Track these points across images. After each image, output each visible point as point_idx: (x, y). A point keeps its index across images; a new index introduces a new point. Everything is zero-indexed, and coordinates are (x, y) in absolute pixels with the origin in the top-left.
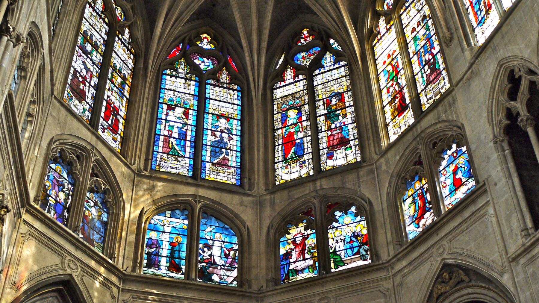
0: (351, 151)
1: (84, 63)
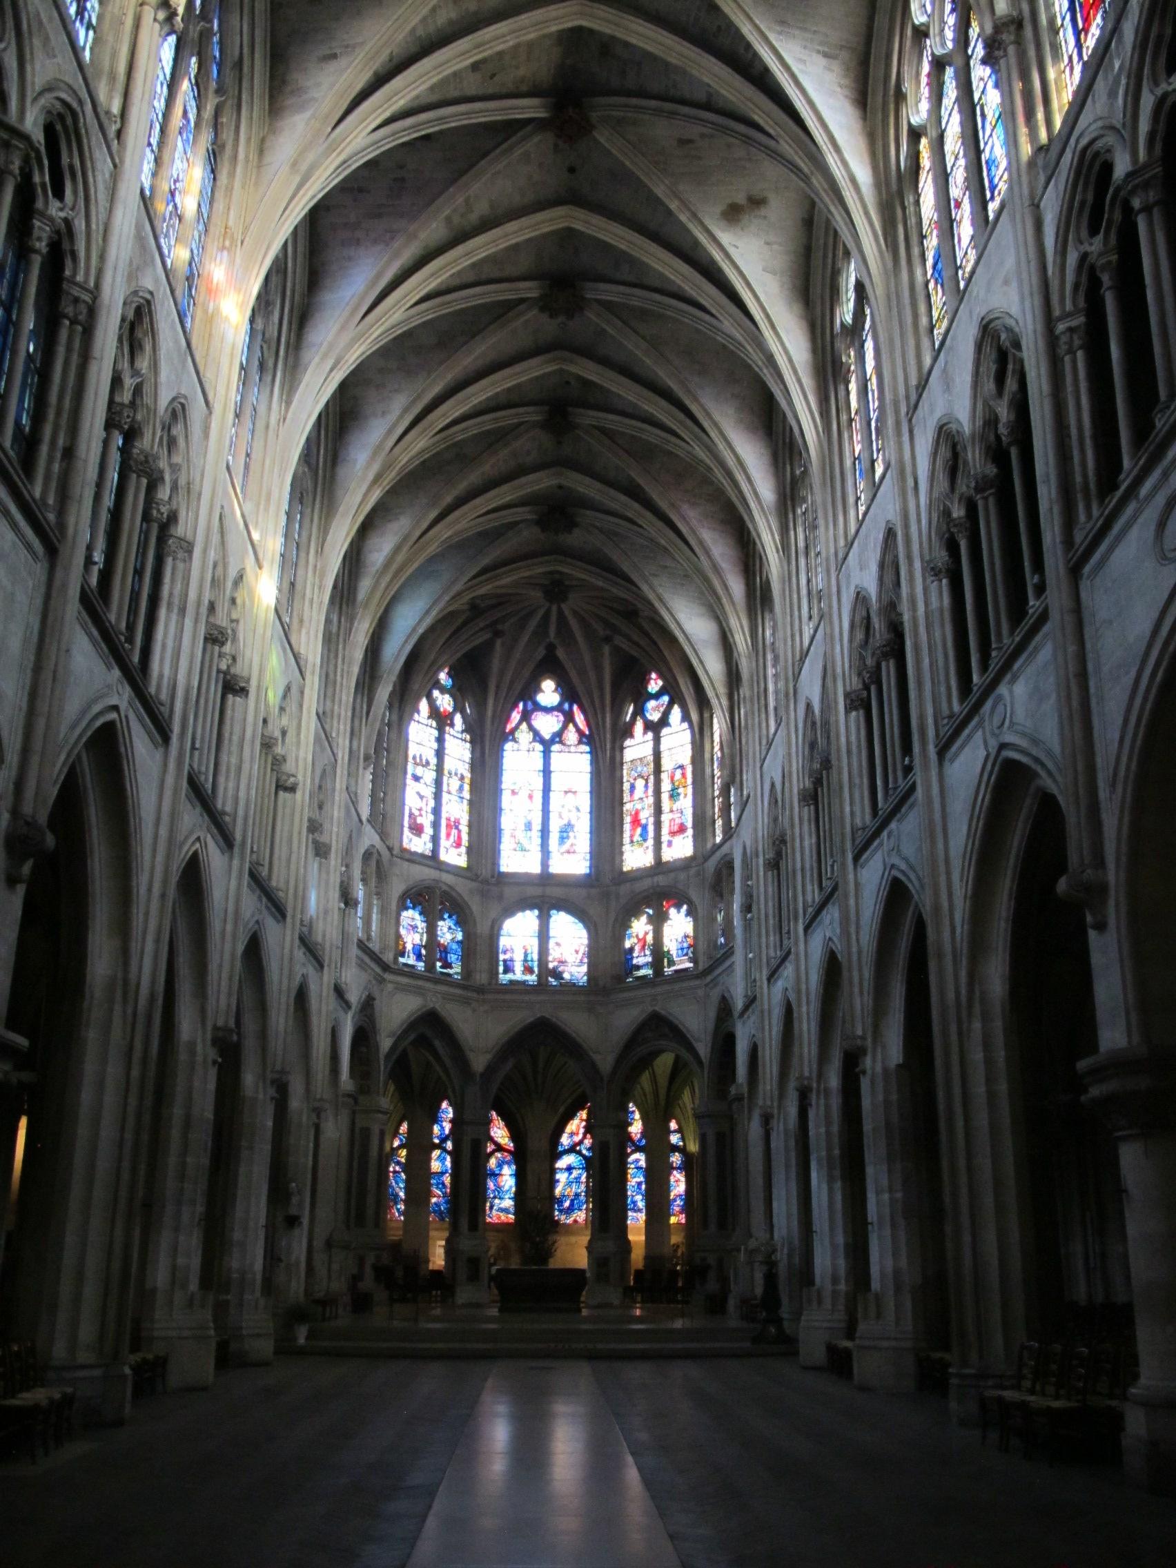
1: (418, 793)
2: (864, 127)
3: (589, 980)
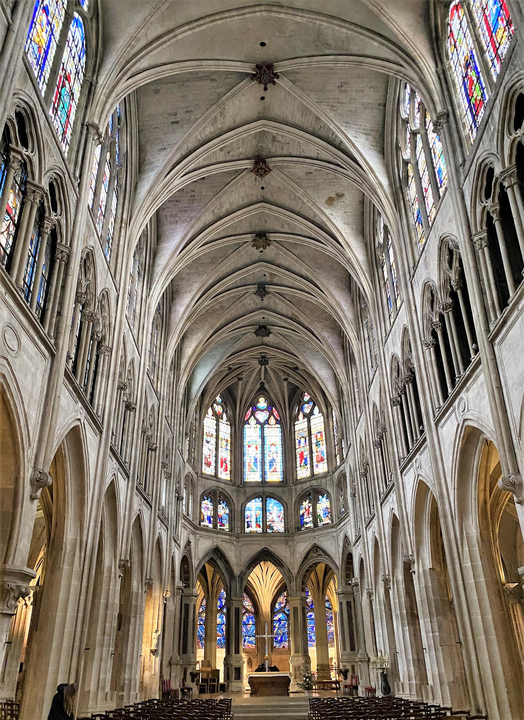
2: (384, 162)
3: (285, 530)
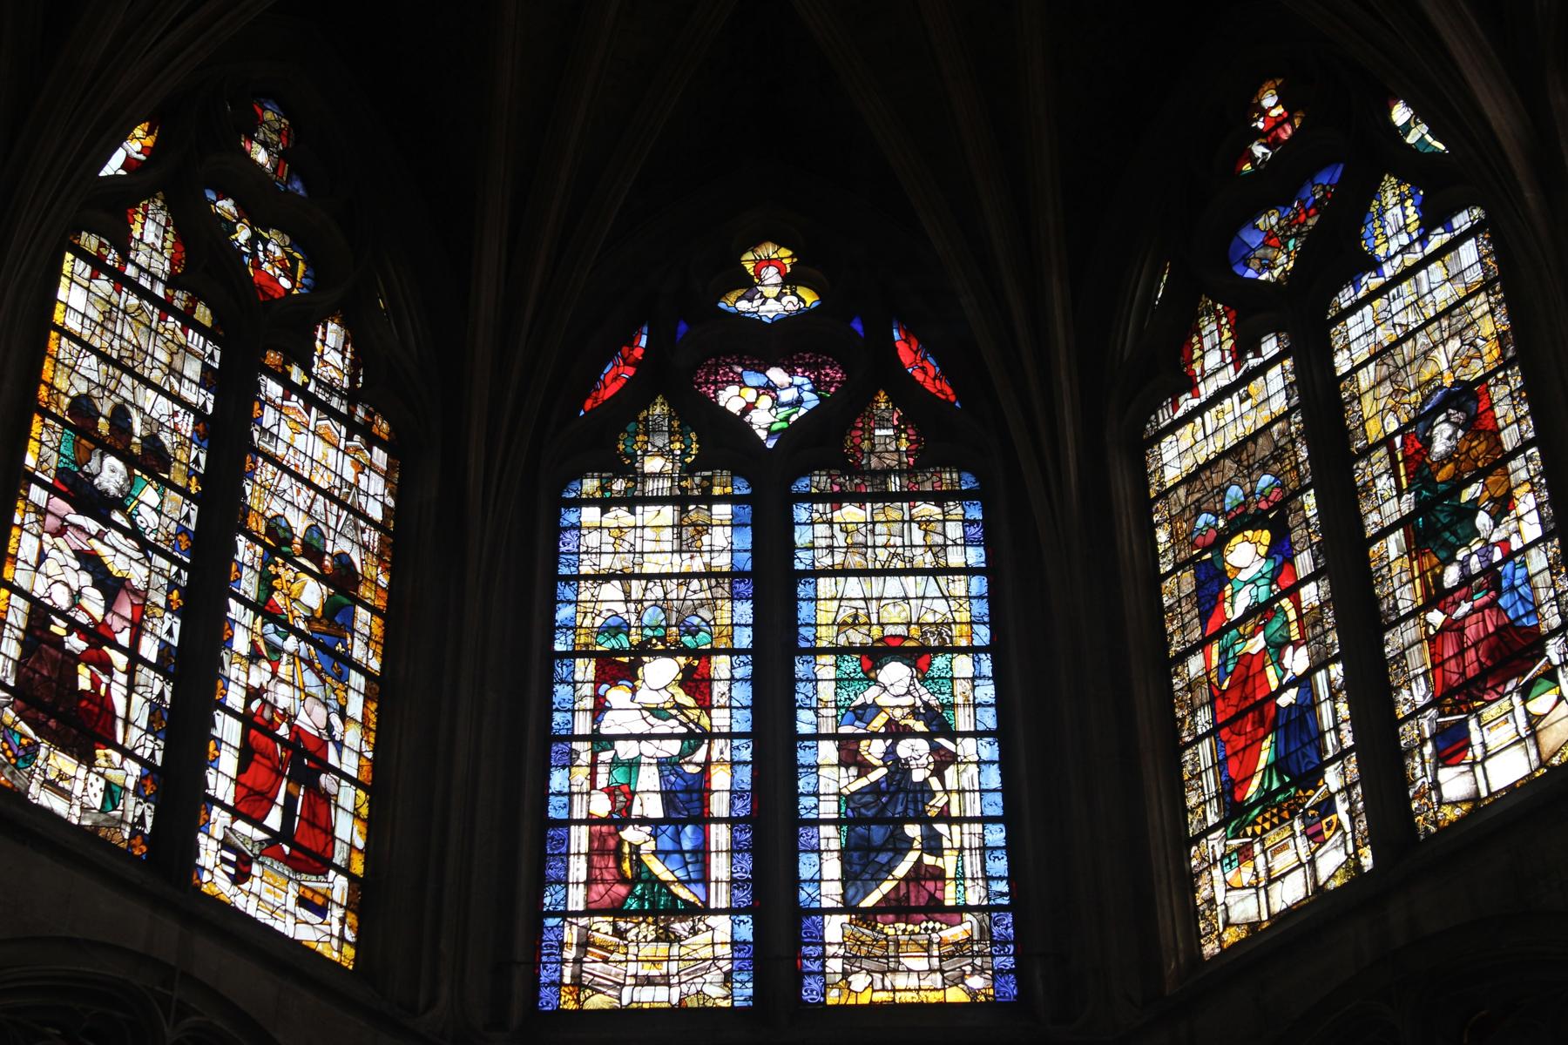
0: (1551, 697)
1: (89, 561)
